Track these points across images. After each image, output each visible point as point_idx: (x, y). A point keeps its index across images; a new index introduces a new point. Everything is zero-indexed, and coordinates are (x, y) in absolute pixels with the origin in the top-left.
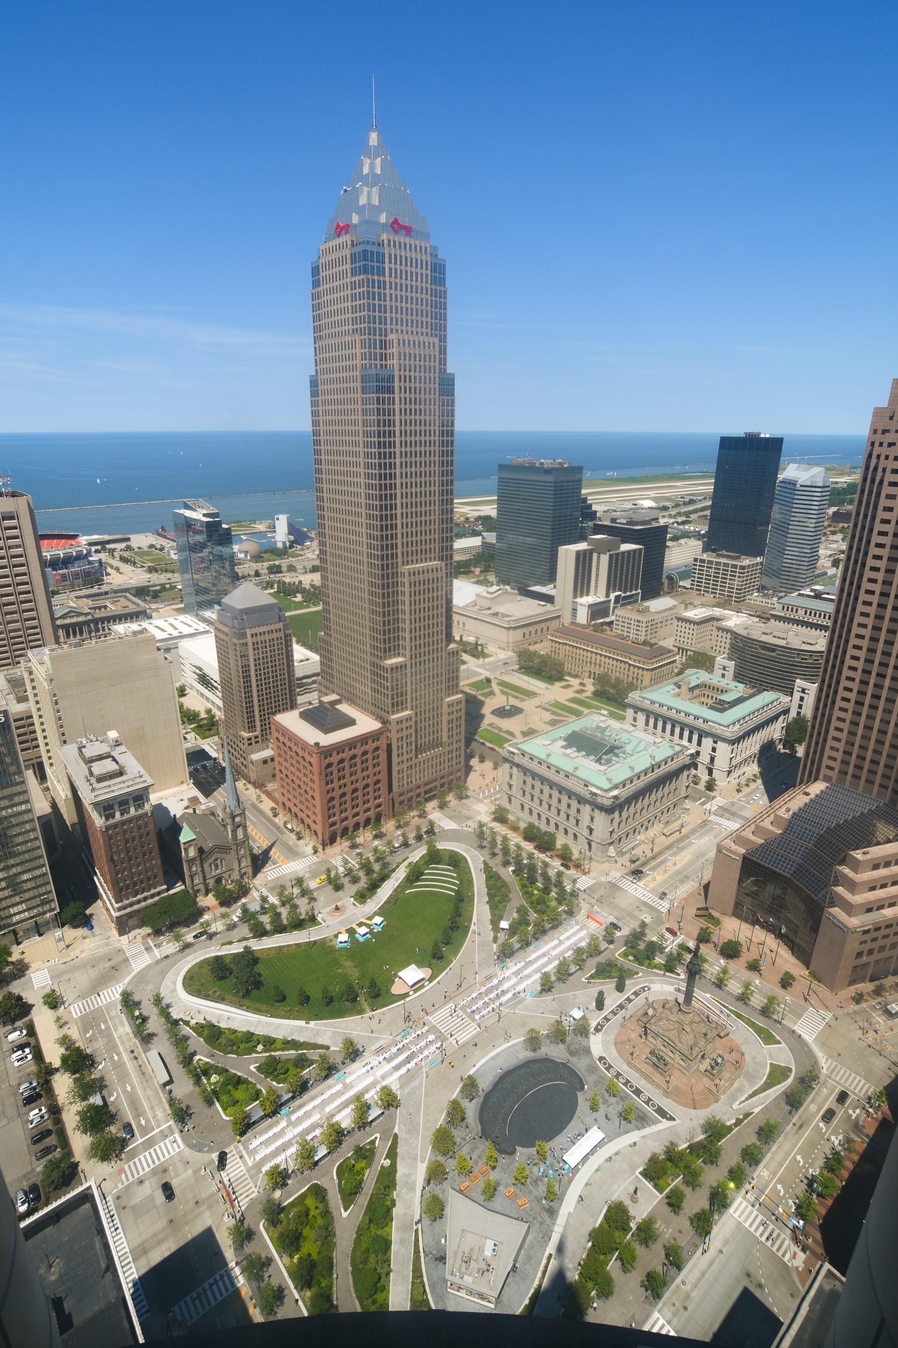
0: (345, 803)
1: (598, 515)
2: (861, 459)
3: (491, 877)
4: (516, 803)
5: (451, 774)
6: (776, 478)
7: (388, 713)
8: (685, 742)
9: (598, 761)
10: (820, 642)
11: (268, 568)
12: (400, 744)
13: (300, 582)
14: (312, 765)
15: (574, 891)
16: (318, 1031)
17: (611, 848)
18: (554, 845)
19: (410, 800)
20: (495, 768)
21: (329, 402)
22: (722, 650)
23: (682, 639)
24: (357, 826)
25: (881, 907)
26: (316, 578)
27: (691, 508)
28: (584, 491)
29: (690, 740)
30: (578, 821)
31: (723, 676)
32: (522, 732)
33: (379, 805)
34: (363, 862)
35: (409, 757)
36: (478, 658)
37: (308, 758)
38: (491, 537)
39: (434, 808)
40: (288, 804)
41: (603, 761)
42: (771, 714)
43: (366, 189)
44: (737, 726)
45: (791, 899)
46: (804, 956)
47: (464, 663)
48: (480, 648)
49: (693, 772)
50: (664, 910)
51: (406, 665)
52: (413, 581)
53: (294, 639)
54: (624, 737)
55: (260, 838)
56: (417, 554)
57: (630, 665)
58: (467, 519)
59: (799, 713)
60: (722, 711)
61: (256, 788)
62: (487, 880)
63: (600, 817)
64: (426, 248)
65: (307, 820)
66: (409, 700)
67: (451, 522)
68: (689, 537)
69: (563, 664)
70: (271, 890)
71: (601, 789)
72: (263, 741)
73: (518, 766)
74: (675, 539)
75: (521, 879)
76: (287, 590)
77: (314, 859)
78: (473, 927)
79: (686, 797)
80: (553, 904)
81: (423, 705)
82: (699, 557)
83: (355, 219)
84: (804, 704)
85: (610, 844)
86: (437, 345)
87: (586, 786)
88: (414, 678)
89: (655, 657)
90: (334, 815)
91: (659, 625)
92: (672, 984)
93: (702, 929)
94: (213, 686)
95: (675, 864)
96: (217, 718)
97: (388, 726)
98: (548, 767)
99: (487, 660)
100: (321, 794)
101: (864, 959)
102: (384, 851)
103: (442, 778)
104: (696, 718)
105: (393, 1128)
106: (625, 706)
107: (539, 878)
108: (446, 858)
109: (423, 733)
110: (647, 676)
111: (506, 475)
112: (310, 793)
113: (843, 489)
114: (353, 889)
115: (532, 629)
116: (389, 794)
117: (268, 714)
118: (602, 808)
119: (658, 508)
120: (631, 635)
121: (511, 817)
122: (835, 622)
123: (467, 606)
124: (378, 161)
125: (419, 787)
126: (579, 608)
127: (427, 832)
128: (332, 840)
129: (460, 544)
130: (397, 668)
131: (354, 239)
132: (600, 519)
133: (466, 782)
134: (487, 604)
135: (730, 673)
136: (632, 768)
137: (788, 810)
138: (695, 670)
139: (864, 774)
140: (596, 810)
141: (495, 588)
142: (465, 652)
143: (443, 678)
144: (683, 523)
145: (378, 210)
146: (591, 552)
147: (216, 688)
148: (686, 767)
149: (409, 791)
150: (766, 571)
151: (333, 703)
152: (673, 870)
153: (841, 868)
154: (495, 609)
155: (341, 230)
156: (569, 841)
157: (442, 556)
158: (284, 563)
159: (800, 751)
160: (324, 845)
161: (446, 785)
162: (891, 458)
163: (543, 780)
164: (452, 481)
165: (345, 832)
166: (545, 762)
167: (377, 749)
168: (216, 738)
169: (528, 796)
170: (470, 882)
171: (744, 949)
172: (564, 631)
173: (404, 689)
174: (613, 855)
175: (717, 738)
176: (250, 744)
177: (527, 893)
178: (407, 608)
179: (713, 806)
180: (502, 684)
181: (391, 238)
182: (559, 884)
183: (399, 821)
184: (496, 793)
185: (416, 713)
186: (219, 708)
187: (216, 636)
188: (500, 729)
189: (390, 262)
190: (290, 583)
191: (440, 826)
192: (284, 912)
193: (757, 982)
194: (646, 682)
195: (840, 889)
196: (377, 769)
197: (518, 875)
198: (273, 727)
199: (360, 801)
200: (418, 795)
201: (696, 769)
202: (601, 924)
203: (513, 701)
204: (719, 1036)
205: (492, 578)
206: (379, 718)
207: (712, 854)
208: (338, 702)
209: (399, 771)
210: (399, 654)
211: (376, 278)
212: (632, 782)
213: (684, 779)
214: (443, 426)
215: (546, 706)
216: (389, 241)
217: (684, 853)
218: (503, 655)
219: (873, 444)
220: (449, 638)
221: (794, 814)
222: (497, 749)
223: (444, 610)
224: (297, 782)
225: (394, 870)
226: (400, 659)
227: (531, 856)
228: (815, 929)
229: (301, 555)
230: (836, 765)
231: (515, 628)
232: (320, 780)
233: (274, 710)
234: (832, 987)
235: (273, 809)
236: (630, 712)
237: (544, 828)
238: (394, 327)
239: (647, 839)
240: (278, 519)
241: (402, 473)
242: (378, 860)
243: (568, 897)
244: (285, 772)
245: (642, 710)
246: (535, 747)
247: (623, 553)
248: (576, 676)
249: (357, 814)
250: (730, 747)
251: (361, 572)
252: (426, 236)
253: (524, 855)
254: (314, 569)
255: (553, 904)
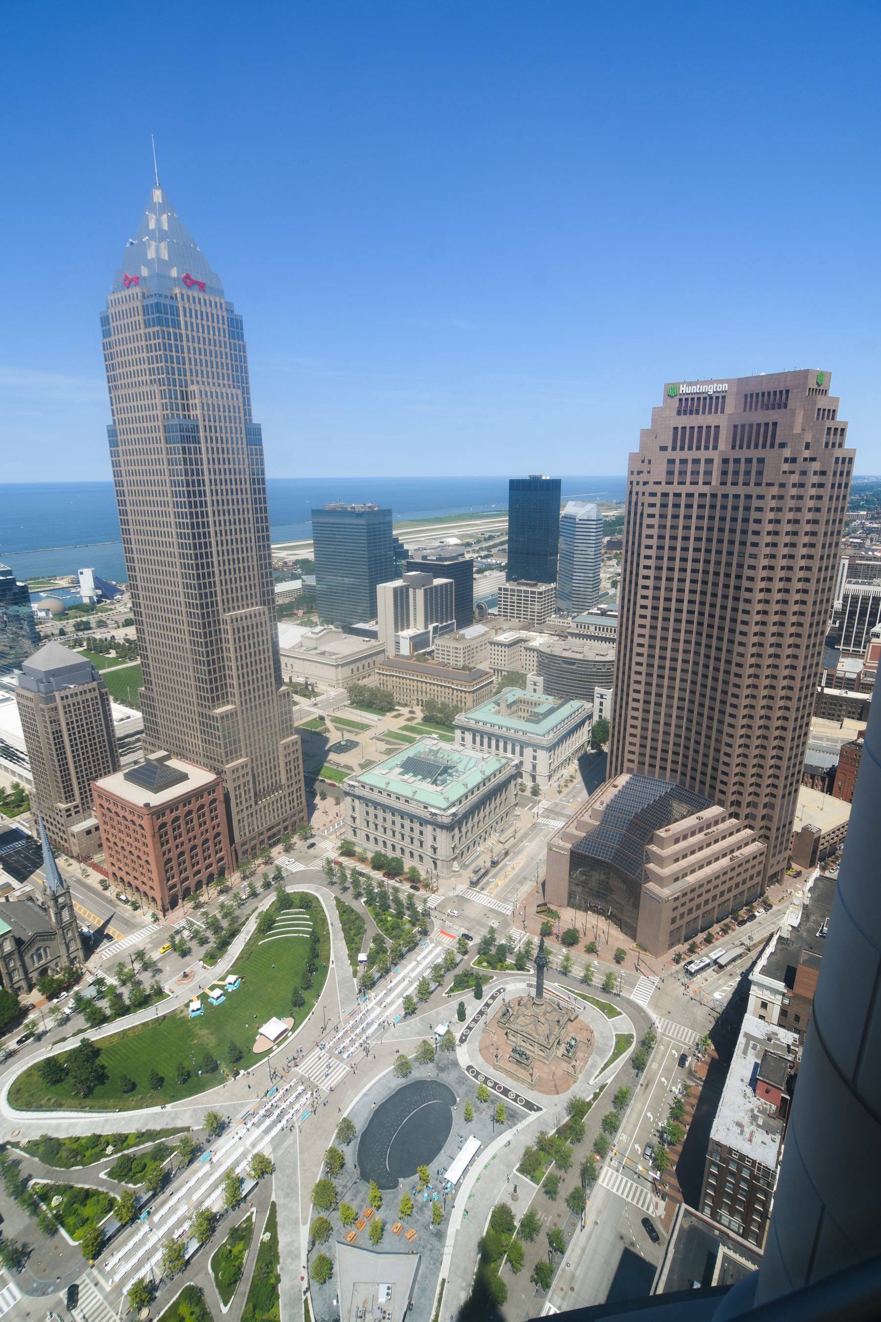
0: (184, 862)
1: (410, 553)
2: (625, 498)
3: (345, 912)
4: (361, 835)
5: (294, 815)
6: (559, 514)
7: (222, 762)
8: (509, 755)
9: (434, 782)
10: (609, 652)
11: (74, 626)
12: (237, 793)
13: (113, 637)
14: (143, 829)
15: (426, 910)
16: (177, 1112)
17: (455, 864)
18: (403, 869)
19: (253, 848)
20: (338, 803)
21: (131, 452)
22: (531, 667)
23: (496, 661)
24: (199, 885)
25: (685, 875)
26: (131, 632)
27: (491, 543)
28: (394, 532)
29: (513, 752)
30: (421, 843)
31: (535, 691)
32: (360, 765)
33: (222, 859)
34: (209, 920)
35: (248, 804)
36: (309, 698)
37: (138, 821)
38: (311, 580)
39: (279, 853)
40: (119, 874)
41: (438, 782)
42: (578, 720)
43: (153, 244)
44: (552, 734)
45: (615, 883)
46: (630, 930)
47: (296, 703)
48: (310, 688)
49: (519, 780)
50: (509, 913)
51: (236, 712)
52: (236, 627)
53: (111, 698)
54: (455, 757)
55: (89, 916)
56: (238, 601)
57: (453, 689)
58: (285, 563)
59: (600, 717)
60: (537, 722)
61: (80, 862)
62: (341, 915)
63: (442, 835)
64: (221, 304)
65: (143, 888)
66: (243, 747)
67: (270, 567)
68: (492, 569)
69: (392, 695)
70: (108, 970)
71: (440, 809)
72: (84, 810)
73: (359, 798)
74: (480, 571)
75: (374, 909)
76: (99, 648)
77: (156, 927)
78: (331, 966)
79: (516, 805)
80: (407, 926)
81: (258, 750)
82: (503, 587)
83: (145, 272)
84: (603, 708)
85: (454, 859)
86: (240, 396)
87: (426, 808)
88: (246, 725)
89: (475, 680)
90: (173, 877)
91: (475, 650)
92: (524, 981)
93: (543, 923)
94: (19, 758)
95: (513, 868)
96: (27, 792)
97: (223, 776)
98: (389, 795)
99: (318, 699)
100: (156, 857)
101: (678, 923)
102: (232, 906)
103: (284, 821)
104: (516, 731)
105: (270, 1197)
106: (452, 728)
107: (393, 905)
108: (297, 901)
109: (260, 778)
110: (470, 698)
111: (321, 520)
112: (144, 858)
113: (613, 521)
114: (202, 951)
115: (360, 664)
116: (231, 845)
117: (88, 780)
118: (442, 827)
119: (462, 545)
120: (451, 662)
121: (358, 849)
122: (621, 635)
123: (294, 647)
124: (164, 217)
125: (262, 834)
126: (401, 641)
127: (275, 878)
128: (173, 904)
129: (280, 588)
130: (227, 716)
131: (145, 291)
132: (412, 557)
133: (309, 821)
134: (313, 644)
135: (540, 687)
136: (465, 785)
137: (602, 803)
138: (511, 688)
139: (658, 763)
140: (437, 830)
141: (319, 628)
142: (296, 693)
143: (277, 721)
144: (486, 557)
145: (169, 265)
146: (407, 588)
147: (23, 760)
148: (513, 777)
149: (251, 840)
150: (560, 595)
151: (161, 760)
152: (511, 874)
153: (650, 847)
154: (322, 648)
155: (130, 282)
156: (416, 863)
157: (264, 601)
158: (92, 619)
159: (606, 748)
160: (165, 911)
161: (290, 828)
162: (647, 494)
163: (385, 808)
164: (267, 527)
165: (186, 893)
166: (385, 790)
167: (214, 801)
168: (27, 815)
169: (372, 825)
170: (324, 921)
171: (581, 935)
172: (390, 664)
173: (237, 737)
174: (457, 869)
175: (536, 747)
176: (69, 816)
177: (381, 921)
178: (232, 655)
179: (539, 809)
180: (336, 720)
181: (184, 292)
182: (411, 906)
183: (244, 872)
184: (340, 828)
185: (252, 760)
186: (28, 781)
187: (19, 703)
188: (338, 765)
189: (185, 315)
190: (101, 640)
191: (287, 870)
192: (126, 992)
193: (596, 962)
194: (469, 703)
195: (651, 866)
196: (215, 822)
197: (370, 905)
198: (95, 794)
199: (200, 857)
200: (262, 842)
201: (521, 778)
202: (454, 937)
203: (348, 736)
204: (570, 1020)
205: (315, 618)
206: (213, 769)
207: (544, 852)
208: (168, 758)
209: (239, 821)
210: (228, 702)
211: (171, 330)
212: (467, 798)
213: (512, 789)
214: (253, 474)
215: (380, 737)
216: (182, 295)
217: (520, 857)
218: (333, 692)
219: (631, 483)
220: (279, 681)
221: (608, 805)
222: (337, 784)
223: (271, 654)
224: (128, 848)
225: (244, 924)
226: (230, 707)
227: (381, 884)
228: (636, 905)
229: (111, 609)
230: (635, 758)
231: (343, 665)
232: (154, 843)
233: (94, 775)
234: (656, 954)
235: (102, 882)
236: (458, 732)
237: (390, 854)
238: (194, 378)
239: (486, 849)
240: (82, 573)
241: (215, 521)
242: (225, 916)
243: (421, 917)
244: (112, 839)
245: (469, 730)
246: (373, 777)
247: (436, 587)
248: (405, 705)
249: (199, 872)
250: (548, 755)
251: (181, 622)
252: (220, 293)
253: (374, 884)
254: (128, 623)
255: (407, 926)
